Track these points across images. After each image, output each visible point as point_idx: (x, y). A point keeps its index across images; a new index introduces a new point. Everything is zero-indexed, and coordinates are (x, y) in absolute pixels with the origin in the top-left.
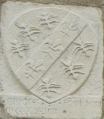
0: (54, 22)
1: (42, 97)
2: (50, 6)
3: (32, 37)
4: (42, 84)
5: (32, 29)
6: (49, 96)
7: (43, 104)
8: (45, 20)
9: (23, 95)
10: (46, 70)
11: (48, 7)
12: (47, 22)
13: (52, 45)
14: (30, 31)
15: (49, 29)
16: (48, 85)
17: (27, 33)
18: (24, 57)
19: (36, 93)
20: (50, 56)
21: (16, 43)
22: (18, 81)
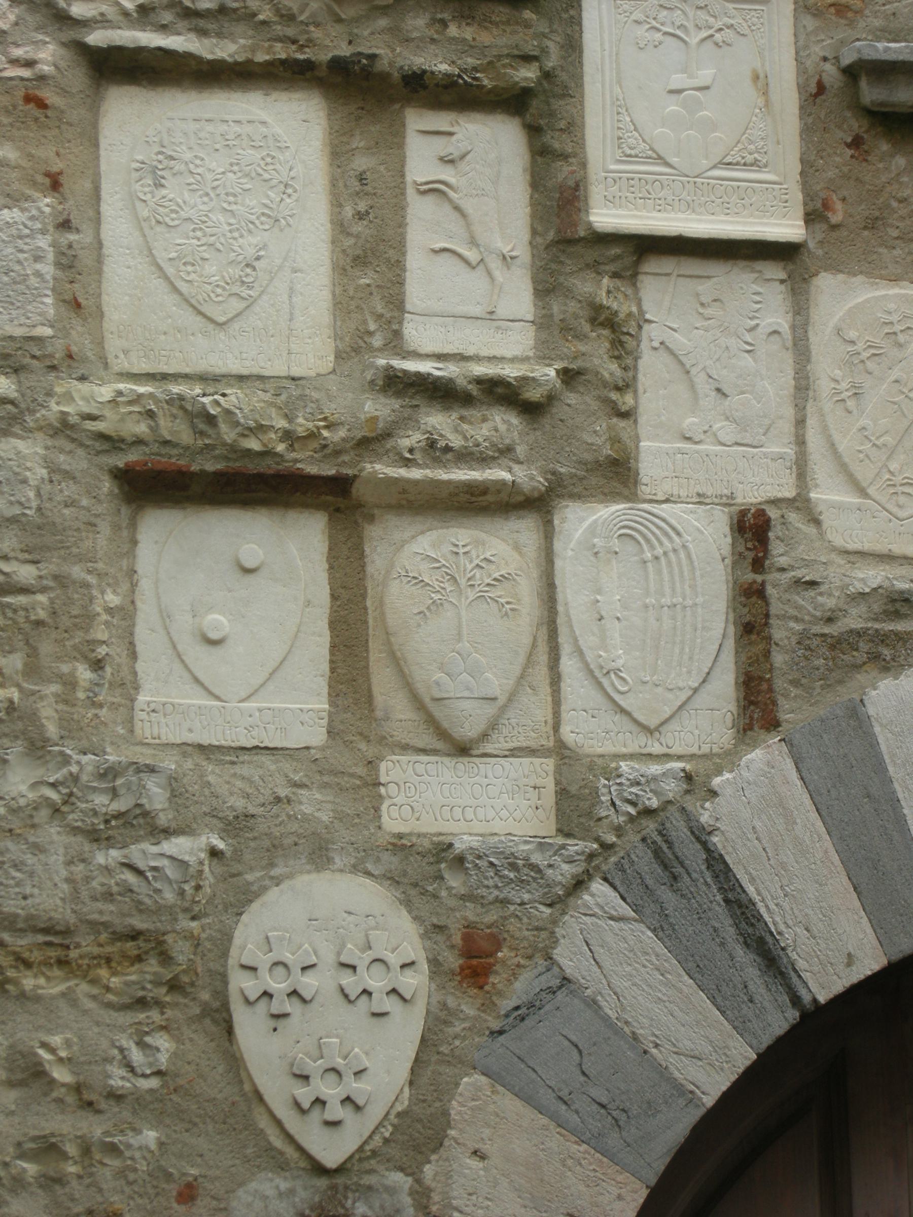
0: (909, 328)
1: (888, 506)
2: (901, 288)
3: (870, 365)
4: (887, 476)
5: (870, 346)
6: (901, 503)
7: (890, 521)
8: (892, 323)
9: (854, 500)
10: (895, 443)
11: (897, 291)
12: (898, 328)
13: (906, 385)
14: (865, 350)
15: (900, 346)
16: (899, 479)
17: (859, 354)
18: (855, 412)
19: (878, 498)
20: (903, 412)
21: (839, 379)
22: (844, 468)
